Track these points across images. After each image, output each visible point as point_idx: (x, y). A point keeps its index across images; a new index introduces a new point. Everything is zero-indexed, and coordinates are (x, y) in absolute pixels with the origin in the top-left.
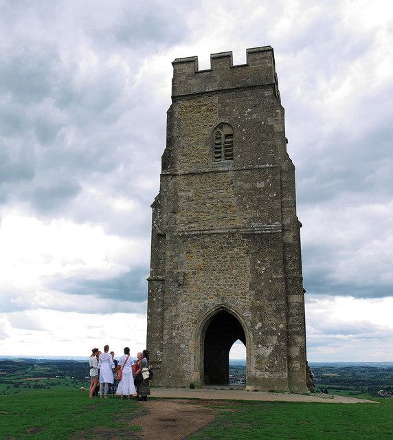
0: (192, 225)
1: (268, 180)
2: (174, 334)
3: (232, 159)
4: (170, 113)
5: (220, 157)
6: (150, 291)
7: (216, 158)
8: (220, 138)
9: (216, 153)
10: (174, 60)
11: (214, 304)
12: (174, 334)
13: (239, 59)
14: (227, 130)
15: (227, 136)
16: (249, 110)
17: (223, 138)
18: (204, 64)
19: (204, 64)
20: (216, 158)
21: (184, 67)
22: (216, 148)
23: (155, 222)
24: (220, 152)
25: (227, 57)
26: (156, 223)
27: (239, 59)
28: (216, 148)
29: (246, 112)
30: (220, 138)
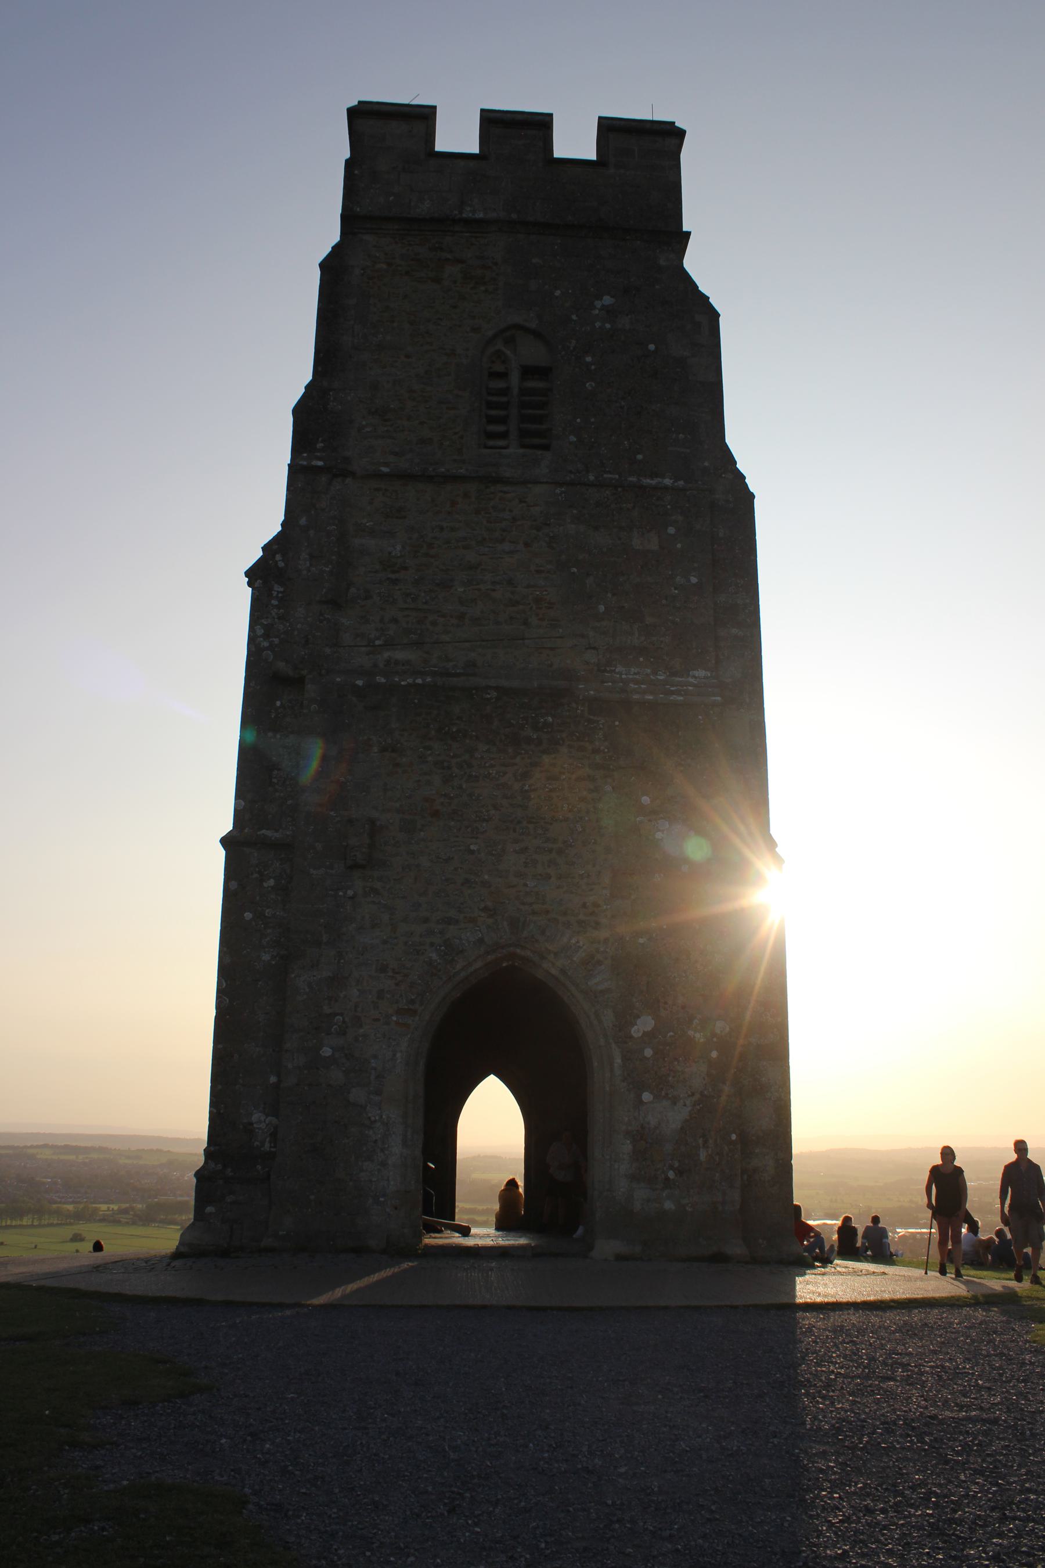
0: (400, 655)
1: (671, 530)
2: (326, 1052)
3: (546, 448)
4: (333, 269)
5: (504, 435)
6: (234, 885)
7: (491, 436)
8: (503, 375)
9: (491, 420)
10: (354, 103)
11: (481, 941)
12: (326, 1052)
13: (575, 142)
14: (532, 352)
15: (528, 372)
16: (607, 300)
17: (515, 379)
18: (457, 135)
19: (457, 135)
20: (491, 436)
21: (385, 138)
22: (490, 405)
23: (260, 631)
24: (503, 420)
25: (539, 126)
26: (266, 636)
27: (575, 142)
28: (490, 405)
29: (598, 304)
30: (503, 375)
